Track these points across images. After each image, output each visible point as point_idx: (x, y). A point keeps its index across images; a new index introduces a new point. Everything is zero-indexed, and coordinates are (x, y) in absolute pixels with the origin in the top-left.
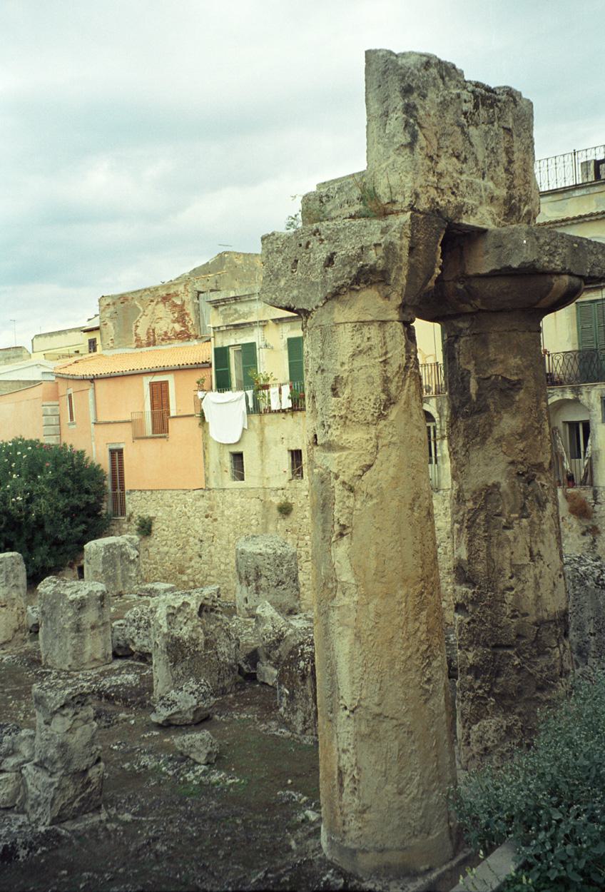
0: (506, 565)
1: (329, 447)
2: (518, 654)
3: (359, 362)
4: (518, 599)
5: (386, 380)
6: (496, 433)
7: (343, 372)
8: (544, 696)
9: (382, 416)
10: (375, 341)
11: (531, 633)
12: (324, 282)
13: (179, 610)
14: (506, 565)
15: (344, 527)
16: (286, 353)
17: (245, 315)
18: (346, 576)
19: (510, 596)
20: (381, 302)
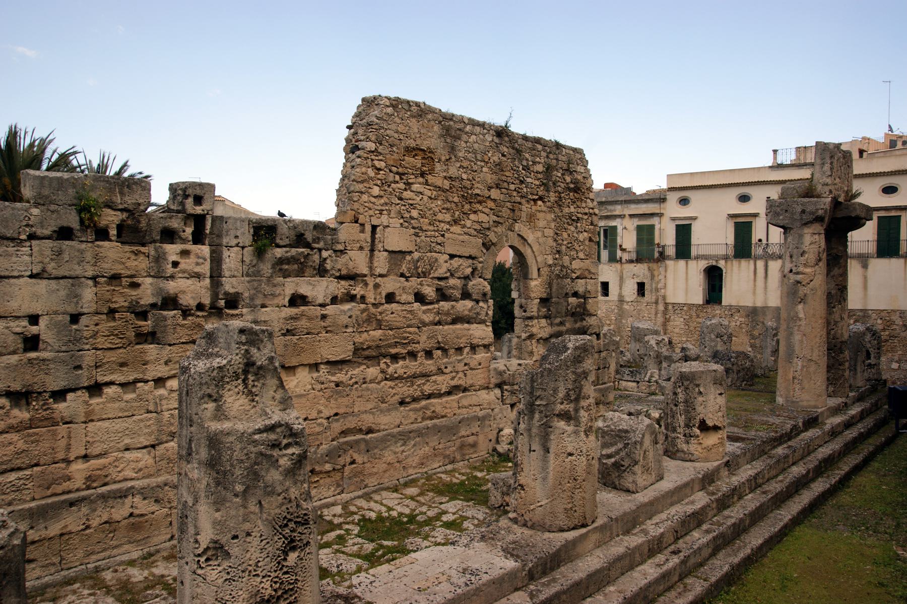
0: (832, 321)
1: (797, 273)
2: (834, 352)
3: (812, 246)
4: (835, 333)
5: (819, 253)
6: (832, 274)
7: (806, 249)
8: (841, 367)
9: (817, 264)
10: (817, 240)
11: (839, 346)
12: (801, 219)
13: (661, 341)
14: (832, 321)
15: (802, 299)
16: (635, 233)
17: (611, 211)
18: (801, 315)
19: (832, 332)
20: (821, 228)
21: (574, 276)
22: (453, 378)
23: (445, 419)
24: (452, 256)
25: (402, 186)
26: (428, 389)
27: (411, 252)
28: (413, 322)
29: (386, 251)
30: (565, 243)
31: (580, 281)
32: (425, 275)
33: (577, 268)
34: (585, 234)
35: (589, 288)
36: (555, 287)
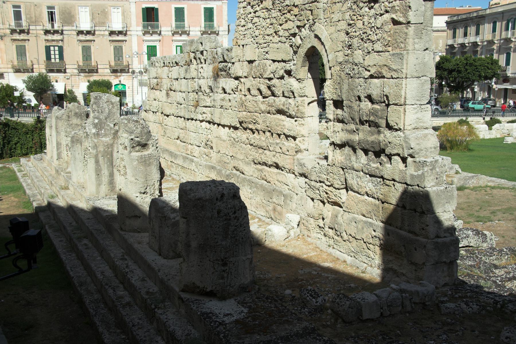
21: (367, 74)
22: (274, 156)
23: (269, 184)
24: (274, 61)
25: (253, 14)
26: (264, 159)
27: (255, 61)
28: (257, 109)
29: (246, 61)
30: (358, 33)
31: (376, 81)
32: (261, 76)
33: (371, 64)
34: (387, 16)
35: (387, 91)
36: (345, 87)
